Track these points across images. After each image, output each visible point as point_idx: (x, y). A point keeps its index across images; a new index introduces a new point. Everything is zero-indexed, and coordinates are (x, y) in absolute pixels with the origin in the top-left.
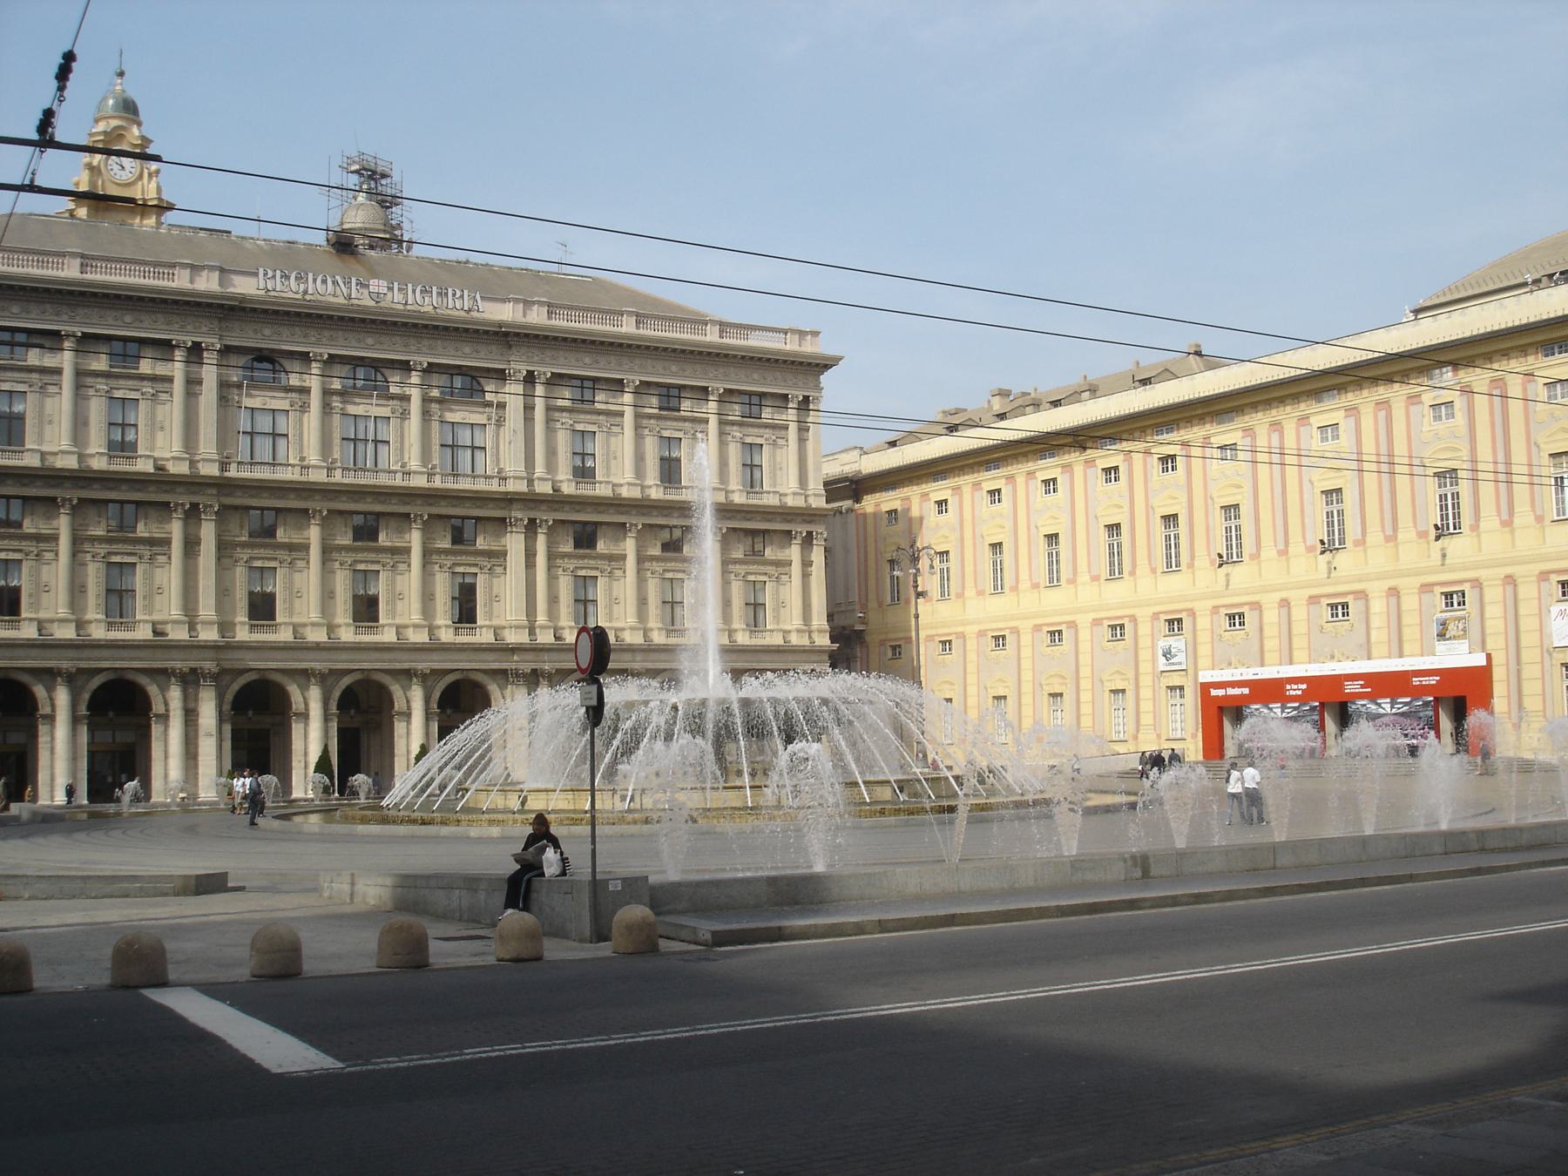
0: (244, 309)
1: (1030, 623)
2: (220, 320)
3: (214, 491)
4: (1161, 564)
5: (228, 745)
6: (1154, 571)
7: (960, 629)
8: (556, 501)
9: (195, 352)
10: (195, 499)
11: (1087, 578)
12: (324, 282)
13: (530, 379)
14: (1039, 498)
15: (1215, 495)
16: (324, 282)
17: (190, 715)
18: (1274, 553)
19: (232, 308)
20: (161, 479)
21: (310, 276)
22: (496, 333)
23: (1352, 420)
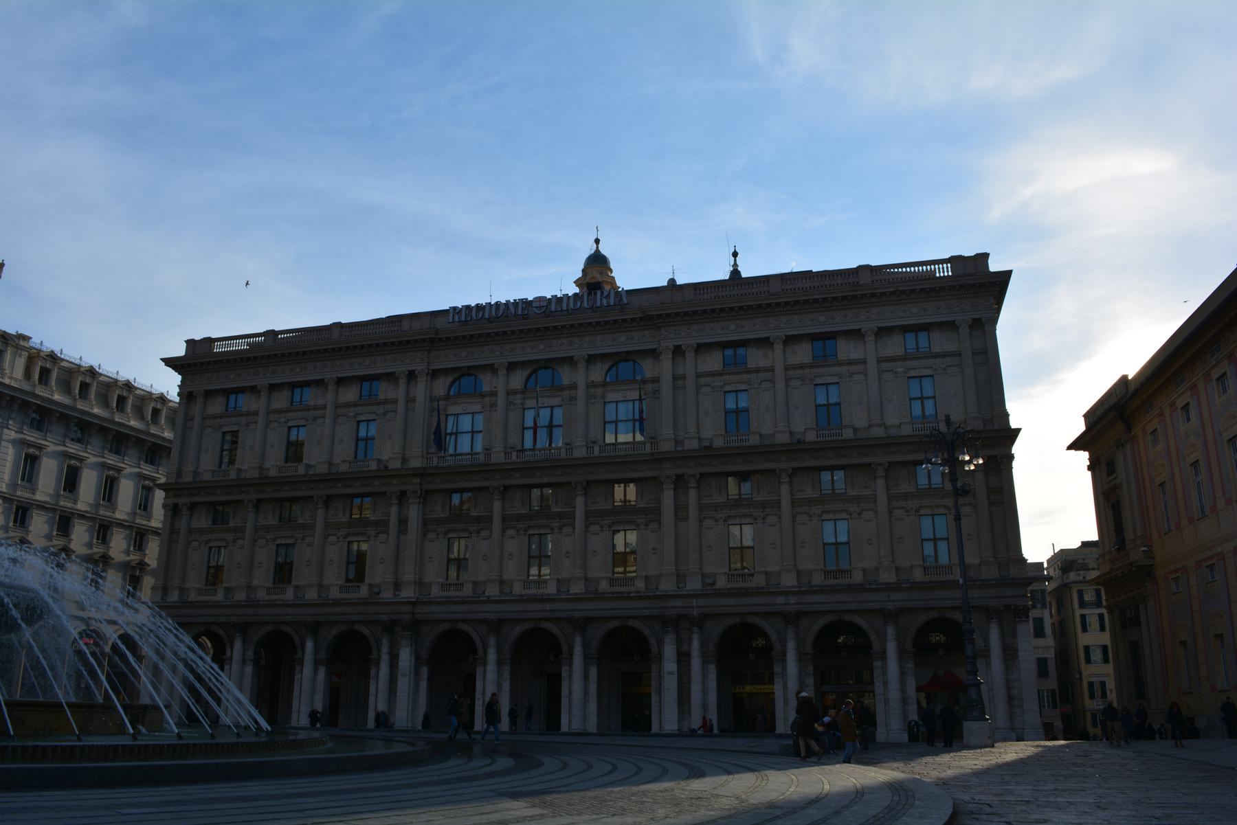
0: (440, 340)
2: (429, 351)
3: (418, 481)
5: (424, 685)
8: (707, 453)
9: (411, 375)
10: (404, 488)
13: (678, 351)
17: (394, 658)
19: (432, 340)
20: (384, 473)
22: (641, 319)
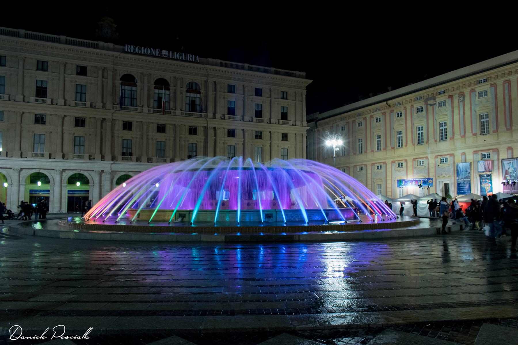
1: (371, 163)
4: (416, 141)
6: (414, 145)
7: (348, 165)
11: (390, 148)
12: (147, 50)
14: (374, 124)
15: (437, 118)
16: (147, 50)
18: (460, 137)
21: (143, 48)
23: (493, 88)
